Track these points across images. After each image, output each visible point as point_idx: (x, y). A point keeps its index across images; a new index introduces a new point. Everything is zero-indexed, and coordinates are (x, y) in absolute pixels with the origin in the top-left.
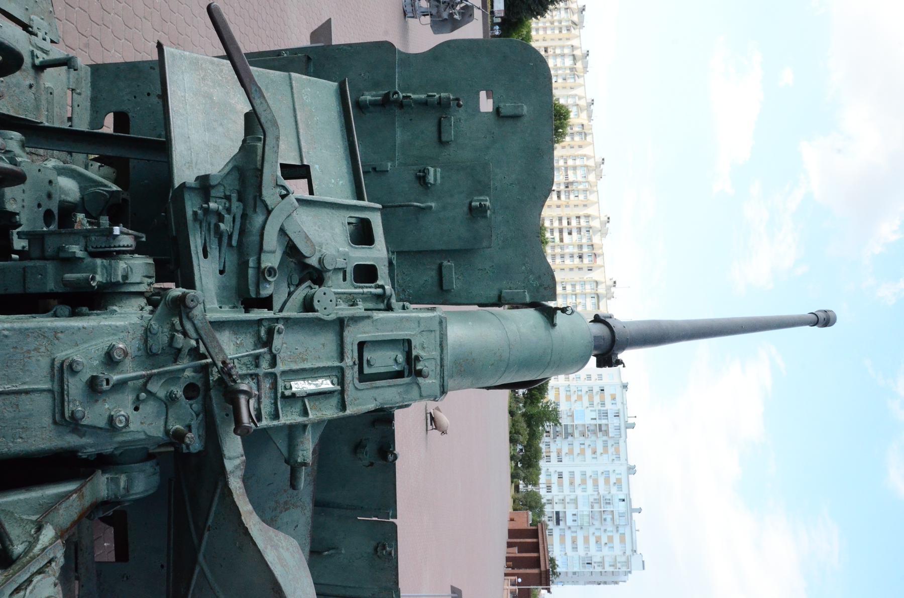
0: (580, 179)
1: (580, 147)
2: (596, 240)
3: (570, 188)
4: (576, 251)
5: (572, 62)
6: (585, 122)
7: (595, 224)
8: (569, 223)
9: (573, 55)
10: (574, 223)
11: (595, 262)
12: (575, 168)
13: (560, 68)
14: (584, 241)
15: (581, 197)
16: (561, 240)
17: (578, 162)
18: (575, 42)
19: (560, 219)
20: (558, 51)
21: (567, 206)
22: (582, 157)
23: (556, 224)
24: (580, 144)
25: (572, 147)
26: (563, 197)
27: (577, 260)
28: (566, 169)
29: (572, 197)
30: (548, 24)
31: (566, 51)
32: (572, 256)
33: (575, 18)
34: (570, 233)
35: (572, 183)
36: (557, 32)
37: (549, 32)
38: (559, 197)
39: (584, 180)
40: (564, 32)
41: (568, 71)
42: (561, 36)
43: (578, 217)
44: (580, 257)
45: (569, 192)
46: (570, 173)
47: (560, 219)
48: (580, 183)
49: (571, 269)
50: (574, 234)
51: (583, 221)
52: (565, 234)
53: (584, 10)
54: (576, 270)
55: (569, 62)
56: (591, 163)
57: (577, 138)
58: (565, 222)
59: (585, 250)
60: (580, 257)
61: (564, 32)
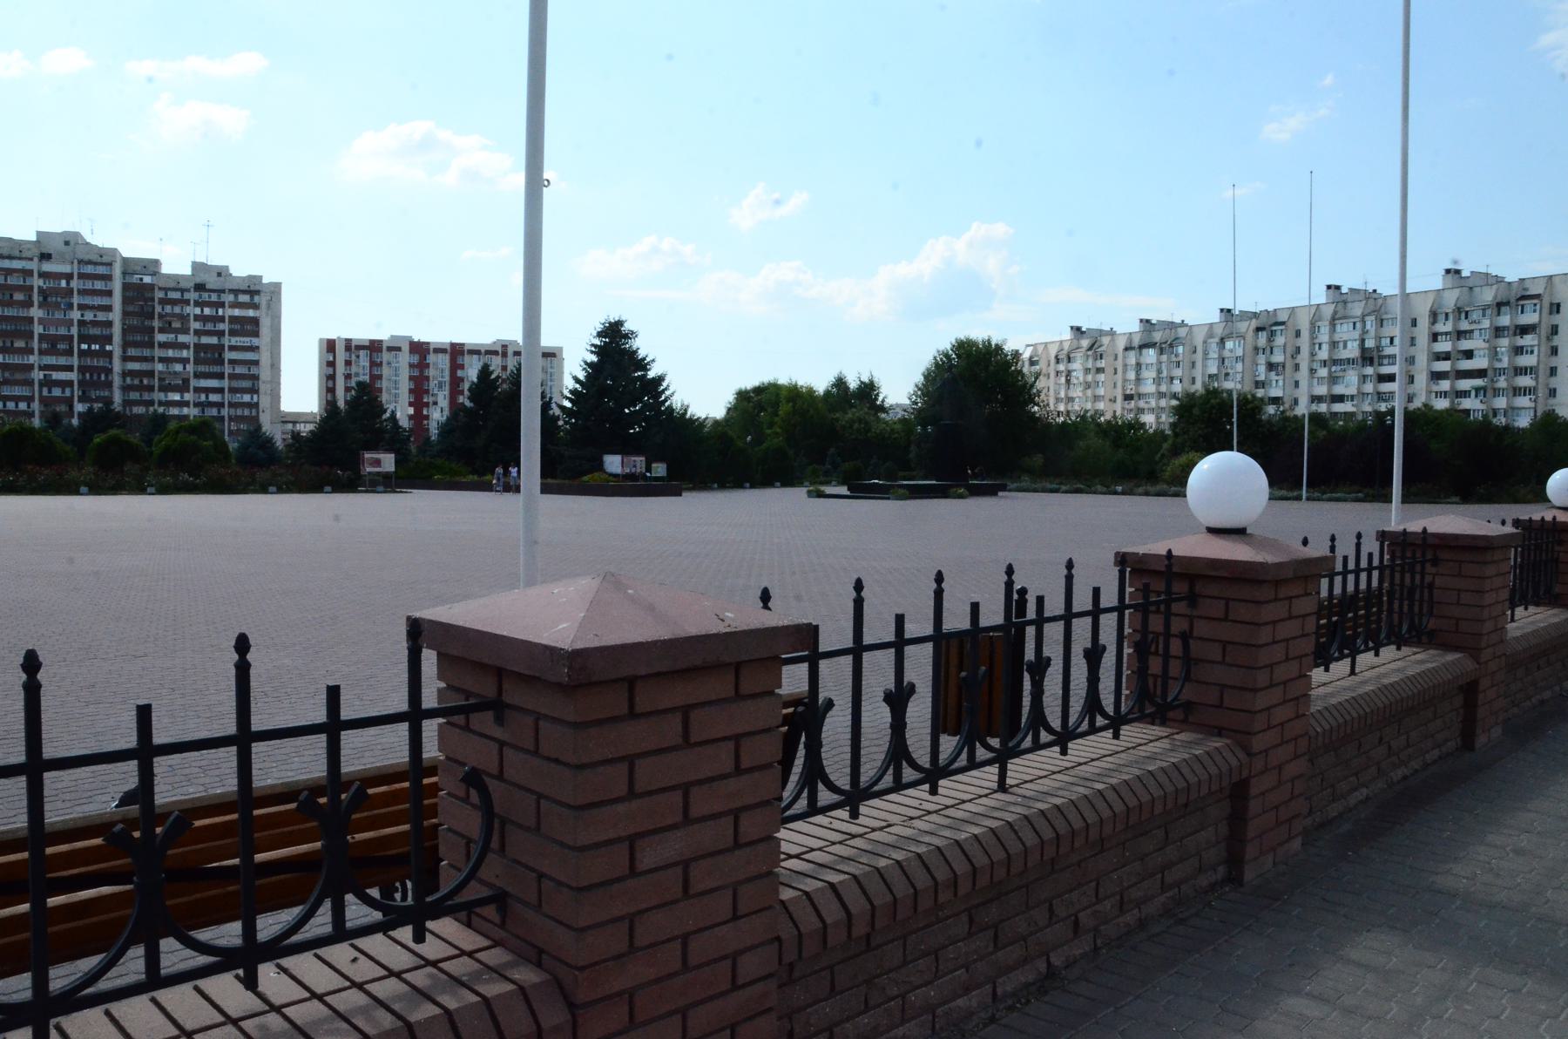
0: (1356, 334)
1: (1298, 334)
2: (1488, 296)
3: (1375, 354)
4: (1504, 343)
5: (1151, 352)
6: (1254, 323)
7: (1450, 299)
8: (1446, 356)
9: (1141, 347)
10: (1444, 346)
11: (1538, 296)
12: (1334, 345)
13: (1159, 372)
14: (1486, 323)
15: (1396, 331)
16: (1481, 373)
17: (1324, 337)
18: (1121, 344)
19: (1437, 376)
20: (1132, 375)
21: (1411, 360)
22: (1314, 328)
23: (1445, 385)
24: (1291, 333)
25: (1298, 350)
26: (1386, 370)
27: (1528, 340)
28: (1335, 362)
29: (1388, 351)
30: (1089, 392)
31: (1132, 360)
32: (1519, 350)
33: (1085, 343)
34: (1469, 354)
35: (1363, 349)
36: (1102, 377)
37: (1101, 391)
38: (1391, 378)
39: (1358, 325)
40: (1101, 364)
41: (1164, 358)
42: (1109, 370)
43: (1435, 337)
44: (1524, 330)
45: (1381, 357)
46: (1344, 354)
47: (1437, 376)
48: (1364, 332)
49: (1554, 351)
50: (1465, 345)
51: (1444, 327)
52: (1466, 365)
53: (1079, 329)
54: (1556, 341)
55: (1150, 355)
56: (1328, 311)
57: (1280, 340)
58: (1444, 366)
59: (1505, 320)
60: (1524, 330)
61: (1101, 364)
